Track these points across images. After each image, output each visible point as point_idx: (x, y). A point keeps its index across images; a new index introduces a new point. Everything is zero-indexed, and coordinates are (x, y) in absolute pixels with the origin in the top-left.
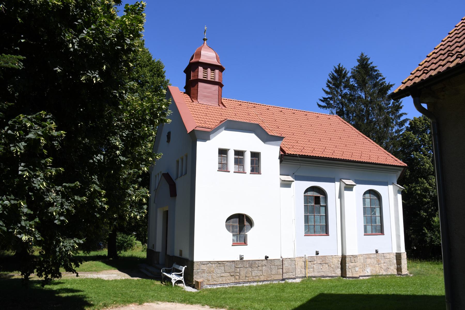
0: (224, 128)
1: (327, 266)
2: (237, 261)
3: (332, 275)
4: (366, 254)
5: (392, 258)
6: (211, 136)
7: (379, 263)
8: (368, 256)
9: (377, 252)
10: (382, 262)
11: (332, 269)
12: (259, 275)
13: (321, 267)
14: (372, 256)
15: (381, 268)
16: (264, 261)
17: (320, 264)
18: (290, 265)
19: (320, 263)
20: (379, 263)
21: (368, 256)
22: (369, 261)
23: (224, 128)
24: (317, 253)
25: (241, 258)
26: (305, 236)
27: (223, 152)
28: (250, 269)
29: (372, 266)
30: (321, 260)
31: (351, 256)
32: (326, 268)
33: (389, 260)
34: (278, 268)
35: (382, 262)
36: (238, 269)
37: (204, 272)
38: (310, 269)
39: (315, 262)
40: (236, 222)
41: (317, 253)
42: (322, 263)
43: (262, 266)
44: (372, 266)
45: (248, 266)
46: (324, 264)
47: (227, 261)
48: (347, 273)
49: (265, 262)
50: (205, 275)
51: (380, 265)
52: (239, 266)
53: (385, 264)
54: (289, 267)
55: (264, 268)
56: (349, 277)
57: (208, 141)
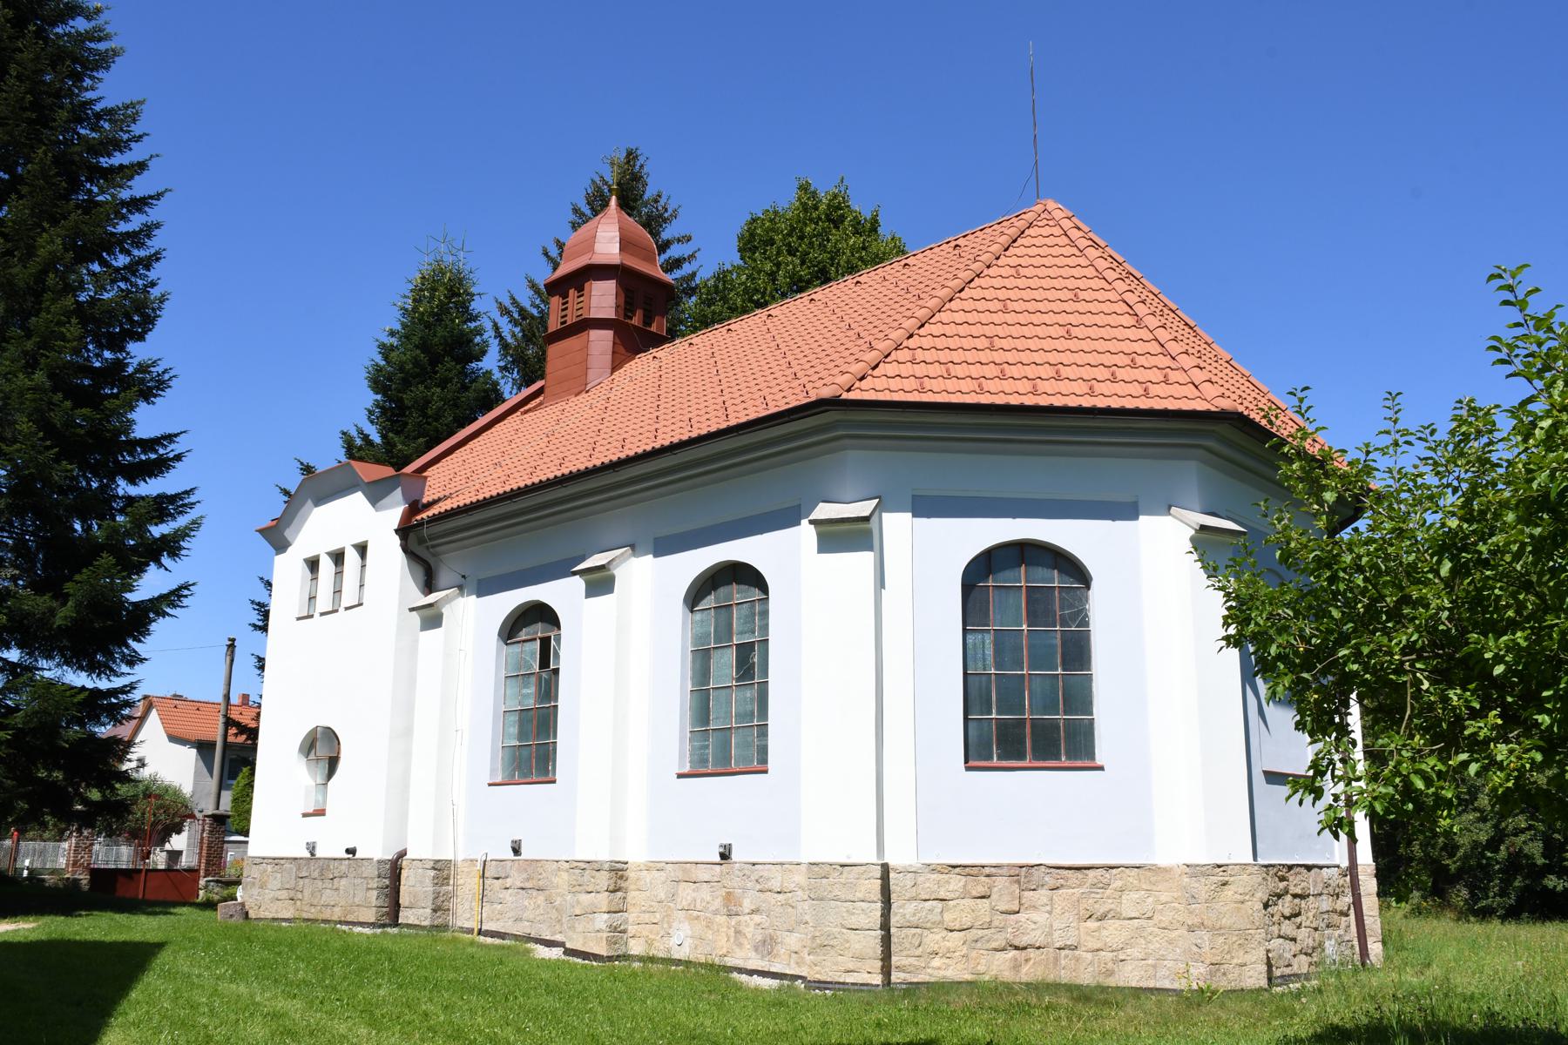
0: (310, 502)
1: (541, 898)
2: (301, 859)
3: (552, 938)
4: (674, 860)
5: (800, 893)
6: (288, 533)
7: (731, 906)
8: (684, 873)
9: (725, 856)
10: (747, 905)
11: (554, 914)
12: (332, 903)
13: (526, 903)
14: (703, 874)
15: (738, 932)
16: (344, 862)
17: (523, 889)
18: (421, 882)
19: (522, 885)
20: (731, 906)
21: (684, 871)
22: (686, 893)
23: (310, 502)
24: (516, 851)
25: (312, 848)
26: (490, 785)
27: (313, 564)
28: (320, 883)
29: (697, 918)
30: (525, 876)
31: (583, 865)
32: (539, 906)
33: (780, 897)
34: (369, 886)
35: (747, 905)
36: (301, 882)
37: (254, 884)
38: (495, 906)
39: (509, 882)
40: (322, 751)
41: (516, 851)
42: (527, 885)
43: (341, 877)
44: (697, 918)
45: (316, 874)
46: (535, 893)
47: (287, 859)
48: (829, 969)
49: (344, 867)
50: (255, 891)
51: (734, 921)
52: (304, 874)
53: (757, 918)
54: (418, 888)
55: (344, 882)
56: (409, 926)
57: (290, 549)
